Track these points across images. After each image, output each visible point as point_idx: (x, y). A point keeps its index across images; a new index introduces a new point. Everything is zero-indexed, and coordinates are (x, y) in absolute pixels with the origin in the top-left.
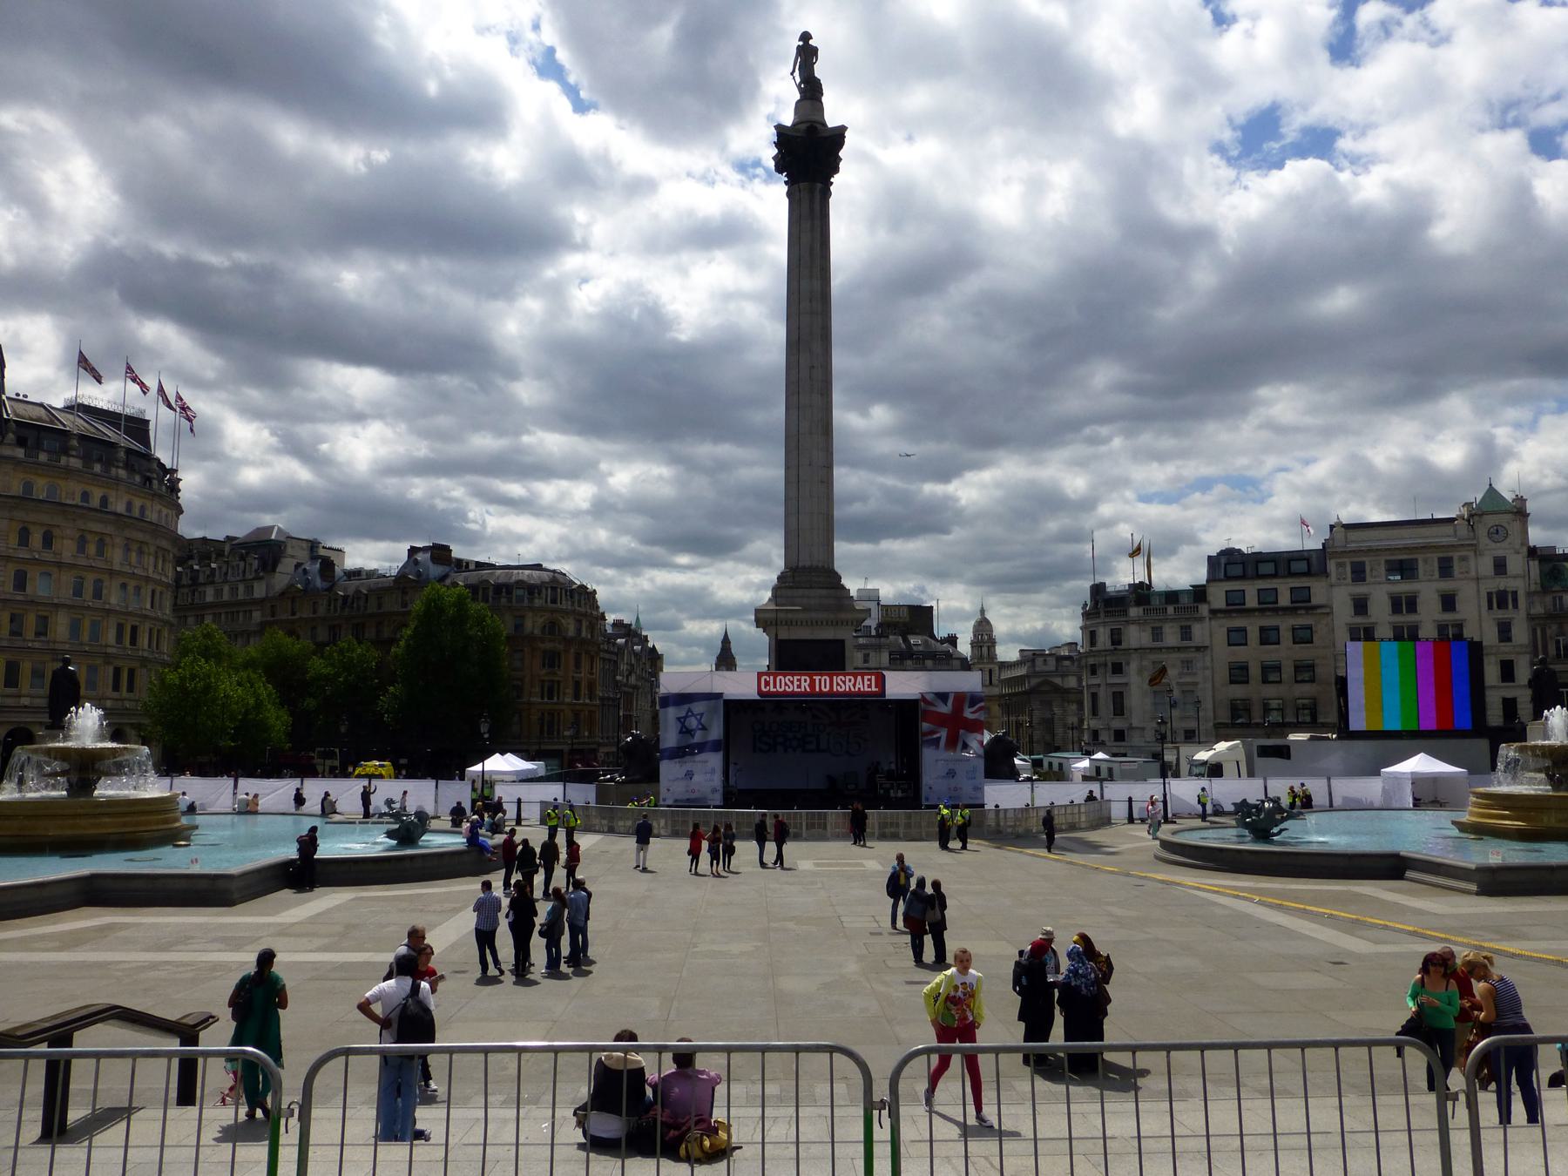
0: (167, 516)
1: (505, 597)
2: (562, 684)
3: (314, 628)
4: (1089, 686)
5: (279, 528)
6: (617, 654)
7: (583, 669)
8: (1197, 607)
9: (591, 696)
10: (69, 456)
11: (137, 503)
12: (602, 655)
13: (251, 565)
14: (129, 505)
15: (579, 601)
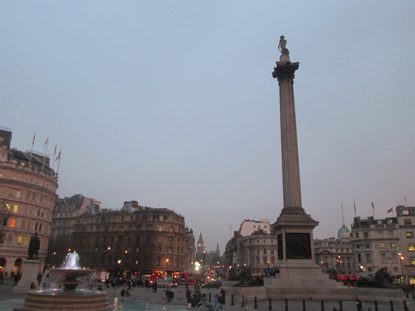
0: (54, 188)
1: (156, 219)
2: (174, 248)
3: (92, 227)
4: (357, 252)
5: (82, 195)
6: (188, 238)
7: (180, 244)
8: (394, 225)
9: (182, 252)
10: (28, 167)
11: (46, 183)
12: (185, 239)
13: (72, 206)
14: (44, 183)
15: (180, 221)
